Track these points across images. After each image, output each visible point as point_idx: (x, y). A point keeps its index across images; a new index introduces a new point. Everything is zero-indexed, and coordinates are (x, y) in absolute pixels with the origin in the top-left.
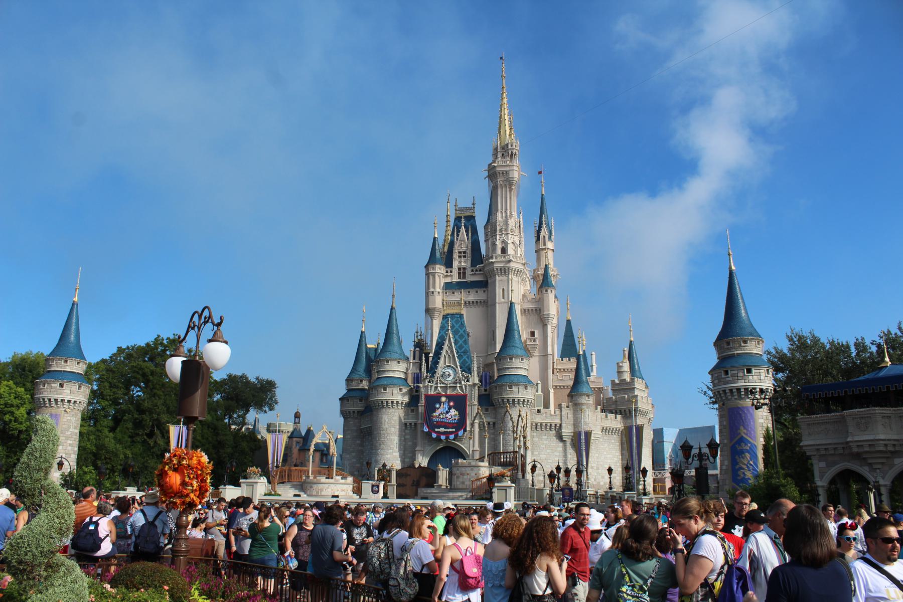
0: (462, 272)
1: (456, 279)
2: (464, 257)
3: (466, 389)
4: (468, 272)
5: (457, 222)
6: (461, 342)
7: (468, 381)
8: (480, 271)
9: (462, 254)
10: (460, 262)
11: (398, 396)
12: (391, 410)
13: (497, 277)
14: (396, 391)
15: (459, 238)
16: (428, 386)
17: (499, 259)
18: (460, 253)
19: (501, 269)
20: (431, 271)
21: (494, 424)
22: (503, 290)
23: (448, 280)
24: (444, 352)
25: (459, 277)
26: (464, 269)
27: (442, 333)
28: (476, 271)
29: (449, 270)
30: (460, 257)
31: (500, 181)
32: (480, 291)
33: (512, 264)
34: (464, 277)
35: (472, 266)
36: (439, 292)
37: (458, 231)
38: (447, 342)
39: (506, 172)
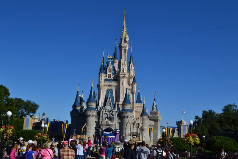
0: (110, 76)
1: (108, 78)
2: (111, 71)
4: (112, 76)
6: (112, 98)
7: (114, 110)
9: (110, 70)
10: (109, 73)
11: (94, 113)
12: (92, 117)
13: (121, 79)
14: (94, 112)
16: (103, 111)
17: (122, 74)
18: (109, 70)
20: (101, 75)
23: (105, 78)
24: (108, 101)
25: (109, 77)
26: (110, 75)
27: (107, 95)
29: (106, 75)
30: (109, 71)
31: (123, 49)
33: (125, 76)
35: (113, 74)
38: (108, 98)
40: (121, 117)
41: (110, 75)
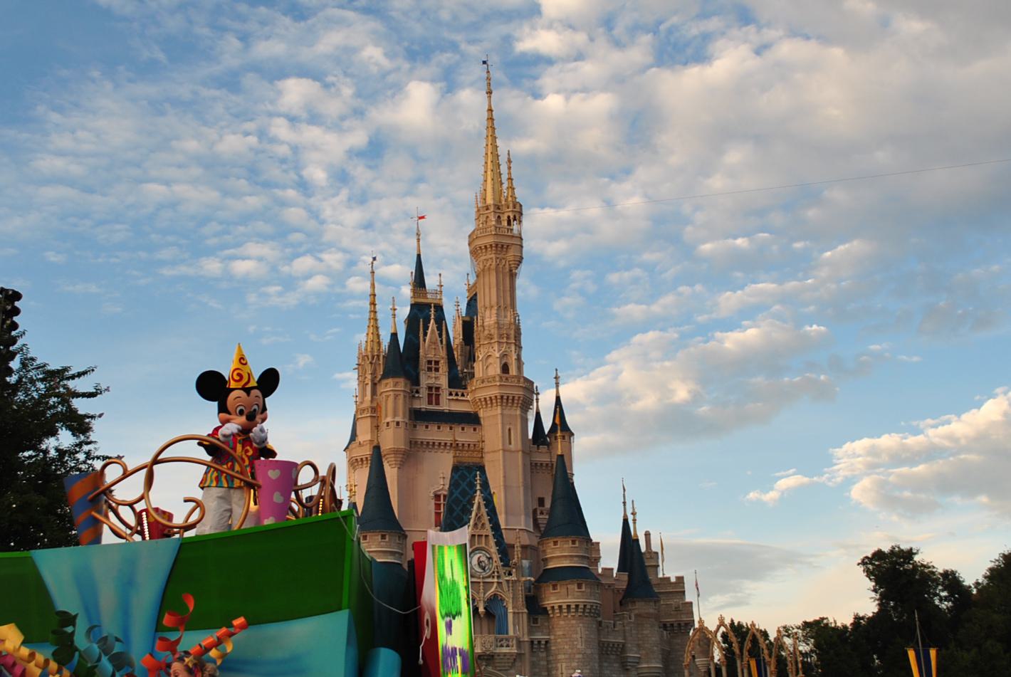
1: (423, 404)
3: (509, 587)
4: (444, 396)
5: (415, 311)
8: (463, 395)
15: (428, 338)
19: (508, 397)
21: (547, 642)
22: (510, 430)
23: (417, 405)
25: (430, 403)
26: (438, 389)
27: (456, 493)
28: (457, 395)
32: (469, 429)
34: (438, 403)
35: (450, 387)
36: (406, 423)
37: (426, 328)
39: (508, 246)
40: (544, 611)
41: (438, 389)
